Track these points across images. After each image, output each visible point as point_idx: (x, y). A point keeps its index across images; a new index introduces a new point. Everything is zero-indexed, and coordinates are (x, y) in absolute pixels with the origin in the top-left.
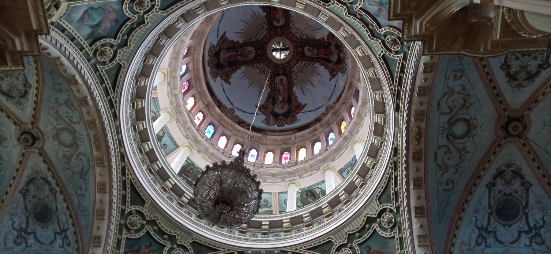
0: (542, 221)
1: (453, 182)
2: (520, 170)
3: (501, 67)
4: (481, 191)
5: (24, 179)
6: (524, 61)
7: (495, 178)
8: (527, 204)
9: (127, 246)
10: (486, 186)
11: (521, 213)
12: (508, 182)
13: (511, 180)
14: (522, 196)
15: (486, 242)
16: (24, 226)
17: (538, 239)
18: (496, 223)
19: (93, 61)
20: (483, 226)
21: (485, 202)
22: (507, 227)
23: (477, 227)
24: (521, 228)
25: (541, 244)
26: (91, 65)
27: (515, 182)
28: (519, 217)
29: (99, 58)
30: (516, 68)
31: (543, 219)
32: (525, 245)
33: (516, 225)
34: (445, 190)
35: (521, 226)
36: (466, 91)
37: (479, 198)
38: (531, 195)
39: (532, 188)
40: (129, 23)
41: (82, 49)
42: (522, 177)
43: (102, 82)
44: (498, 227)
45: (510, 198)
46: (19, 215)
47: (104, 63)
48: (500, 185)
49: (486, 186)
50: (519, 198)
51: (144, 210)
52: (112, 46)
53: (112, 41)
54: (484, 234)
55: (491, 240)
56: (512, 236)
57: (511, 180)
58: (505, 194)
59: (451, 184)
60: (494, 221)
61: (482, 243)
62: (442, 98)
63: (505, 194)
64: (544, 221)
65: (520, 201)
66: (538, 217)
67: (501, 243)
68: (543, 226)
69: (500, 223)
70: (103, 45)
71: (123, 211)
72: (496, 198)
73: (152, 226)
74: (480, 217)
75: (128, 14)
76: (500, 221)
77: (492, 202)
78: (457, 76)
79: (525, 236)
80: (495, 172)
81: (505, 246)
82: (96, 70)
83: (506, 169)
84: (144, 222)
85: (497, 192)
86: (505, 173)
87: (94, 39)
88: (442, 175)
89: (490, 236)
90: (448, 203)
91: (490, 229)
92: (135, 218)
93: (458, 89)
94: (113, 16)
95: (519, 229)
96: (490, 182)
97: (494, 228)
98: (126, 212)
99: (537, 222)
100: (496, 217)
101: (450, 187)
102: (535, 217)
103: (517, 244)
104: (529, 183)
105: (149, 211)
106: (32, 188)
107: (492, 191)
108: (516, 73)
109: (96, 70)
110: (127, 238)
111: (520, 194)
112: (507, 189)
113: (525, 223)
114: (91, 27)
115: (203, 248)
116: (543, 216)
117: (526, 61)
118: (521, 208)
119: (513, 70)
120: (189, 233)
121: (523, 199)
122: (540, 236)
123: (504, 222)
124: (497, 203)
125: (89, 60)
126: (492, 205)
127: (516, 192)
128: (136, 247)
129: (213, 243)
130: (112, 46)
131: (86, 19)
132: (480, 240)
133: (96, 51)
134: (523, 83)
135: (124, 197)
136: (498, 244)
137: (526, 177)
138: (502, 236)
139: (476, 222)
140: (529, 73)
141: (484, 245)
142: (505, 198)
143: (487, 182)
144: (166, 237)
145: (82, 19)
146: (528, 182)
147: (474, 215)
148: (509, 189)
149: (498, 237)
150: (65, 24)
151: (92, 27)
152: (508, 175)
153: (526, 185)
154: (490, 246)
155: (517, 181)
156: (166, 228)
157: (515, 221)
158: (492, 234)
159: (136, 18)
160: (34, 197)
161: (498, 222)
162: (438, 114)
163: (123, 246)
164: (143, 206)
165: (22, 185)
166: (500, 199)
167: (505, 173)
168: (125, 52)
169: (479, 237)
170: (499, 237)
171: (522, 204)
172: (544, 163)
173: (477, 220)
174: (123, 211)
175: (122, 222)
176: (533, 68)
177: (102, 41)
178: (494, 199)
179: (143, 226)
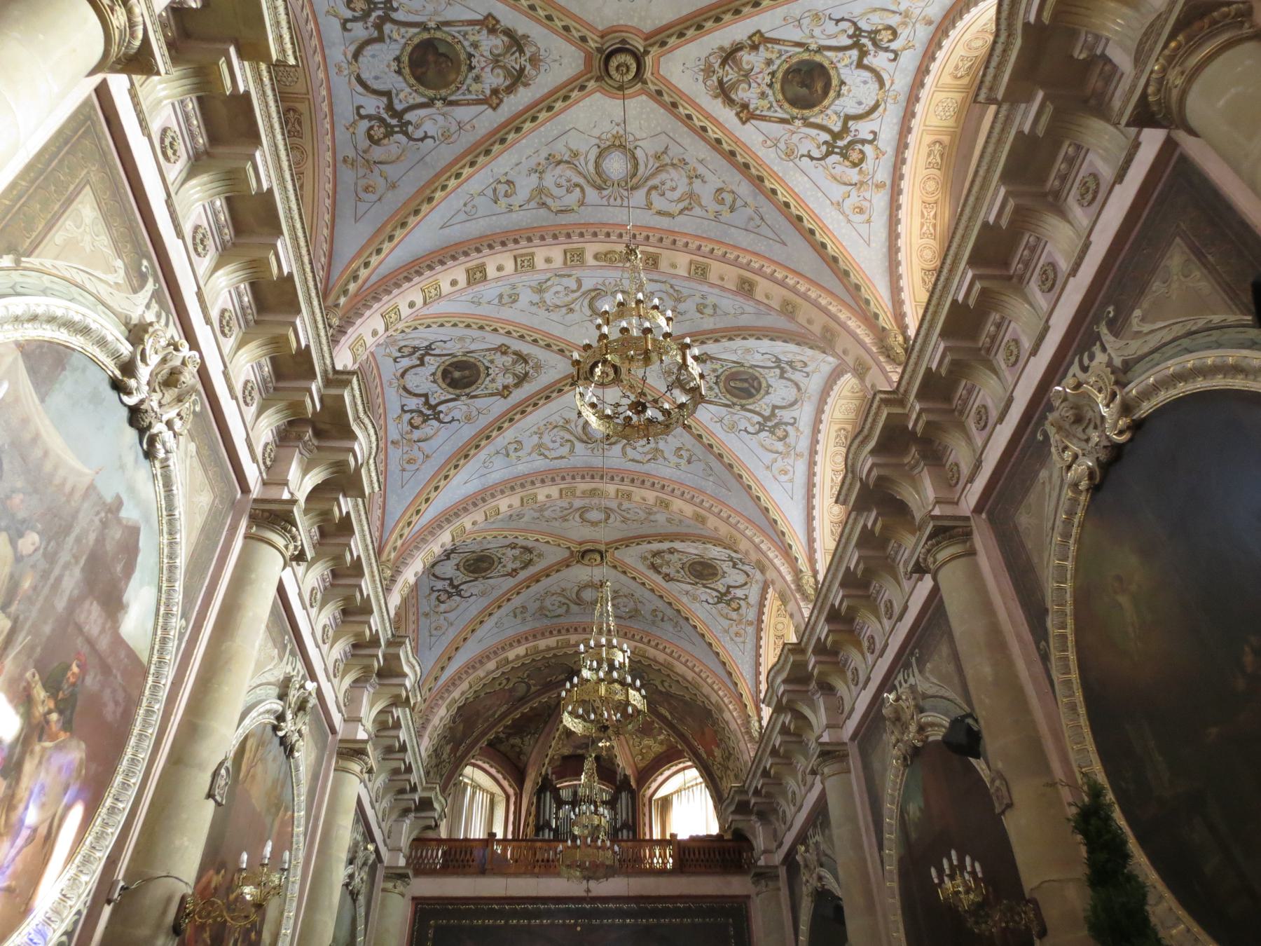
0: (422, 135)
2: (526, 85)
3: (759, 31)
6: (760, 76)
7: (508, 33)
8: (452, 103)
10: (490, 15)
11: (431, 93)
12: (497, 61)
13: (504, 67)
14: (470, 92)
15: (355, 19)
17: (379, 132)
18: (403, 41)
20: (396, 10)
22: (394, 66)
24: (397, 95)
25: (370, 137)
27: (498, 75)
28: (422, 89)
30: (748, 63)
31: (426, 137)
32: (359, 108)
33: (404, 85)
35: (402, 96)
39: (490, 110)
42: (510, 90)
45: (464, 68)
48: (490, 44)
49: (490, 15)
50: (465, 87)
54: (374, 15)
56: (376, 78)
57: (504, 67)
58: (470, 56)
60: (409, 35)
61: (354, 10)
63: (470, 56)
64: (422, 140)
65: (458, 88)
66: (429, 127)
67: (356, 56)
68: (410, 138)
72: (461, 38)
76: (409, 49)
79: (382, 106)
80: (520, 32)
83: (528, 55)
85: (476, 38)
89: (372, 30)
91: (388, 27)
95: (394, 91)
97: (390, 38)
99: (417, 127)
100: (416, 41)
102: (428, 121)
103: (360, 89)
104: (498, 105)
107: (477, 28)
108: (738, 64)
111: (474, 87)
112: (482, 59)
113: (411, 102)
116: (433, 137)
117: (759, 81)
118: (443, 92)
119: (746, 57)
121: (464, 94)
122: (387, 135)
123: (405, 59)
124: (449, 39)
126: (445, 29)
127: (477, 79)
134: (715, 78)
136: (352, 48)
137: (512, 96)
138: (373, 56)
140: (734, 86)
142: (463, 56)
143: (499, 17)
146: (501, 101)
148: (483, 64)
149: (369, 48)
152: (512, 61)
153: (493, 99)
154: (345, 28)
155: (501, 80)
157: (412, 81)
158: (376, 34)
166: (458, 47)
170: (369, 50)
171: (453, 93)
172: (542, 129)
176: (744, 94)
178: (459, 32)
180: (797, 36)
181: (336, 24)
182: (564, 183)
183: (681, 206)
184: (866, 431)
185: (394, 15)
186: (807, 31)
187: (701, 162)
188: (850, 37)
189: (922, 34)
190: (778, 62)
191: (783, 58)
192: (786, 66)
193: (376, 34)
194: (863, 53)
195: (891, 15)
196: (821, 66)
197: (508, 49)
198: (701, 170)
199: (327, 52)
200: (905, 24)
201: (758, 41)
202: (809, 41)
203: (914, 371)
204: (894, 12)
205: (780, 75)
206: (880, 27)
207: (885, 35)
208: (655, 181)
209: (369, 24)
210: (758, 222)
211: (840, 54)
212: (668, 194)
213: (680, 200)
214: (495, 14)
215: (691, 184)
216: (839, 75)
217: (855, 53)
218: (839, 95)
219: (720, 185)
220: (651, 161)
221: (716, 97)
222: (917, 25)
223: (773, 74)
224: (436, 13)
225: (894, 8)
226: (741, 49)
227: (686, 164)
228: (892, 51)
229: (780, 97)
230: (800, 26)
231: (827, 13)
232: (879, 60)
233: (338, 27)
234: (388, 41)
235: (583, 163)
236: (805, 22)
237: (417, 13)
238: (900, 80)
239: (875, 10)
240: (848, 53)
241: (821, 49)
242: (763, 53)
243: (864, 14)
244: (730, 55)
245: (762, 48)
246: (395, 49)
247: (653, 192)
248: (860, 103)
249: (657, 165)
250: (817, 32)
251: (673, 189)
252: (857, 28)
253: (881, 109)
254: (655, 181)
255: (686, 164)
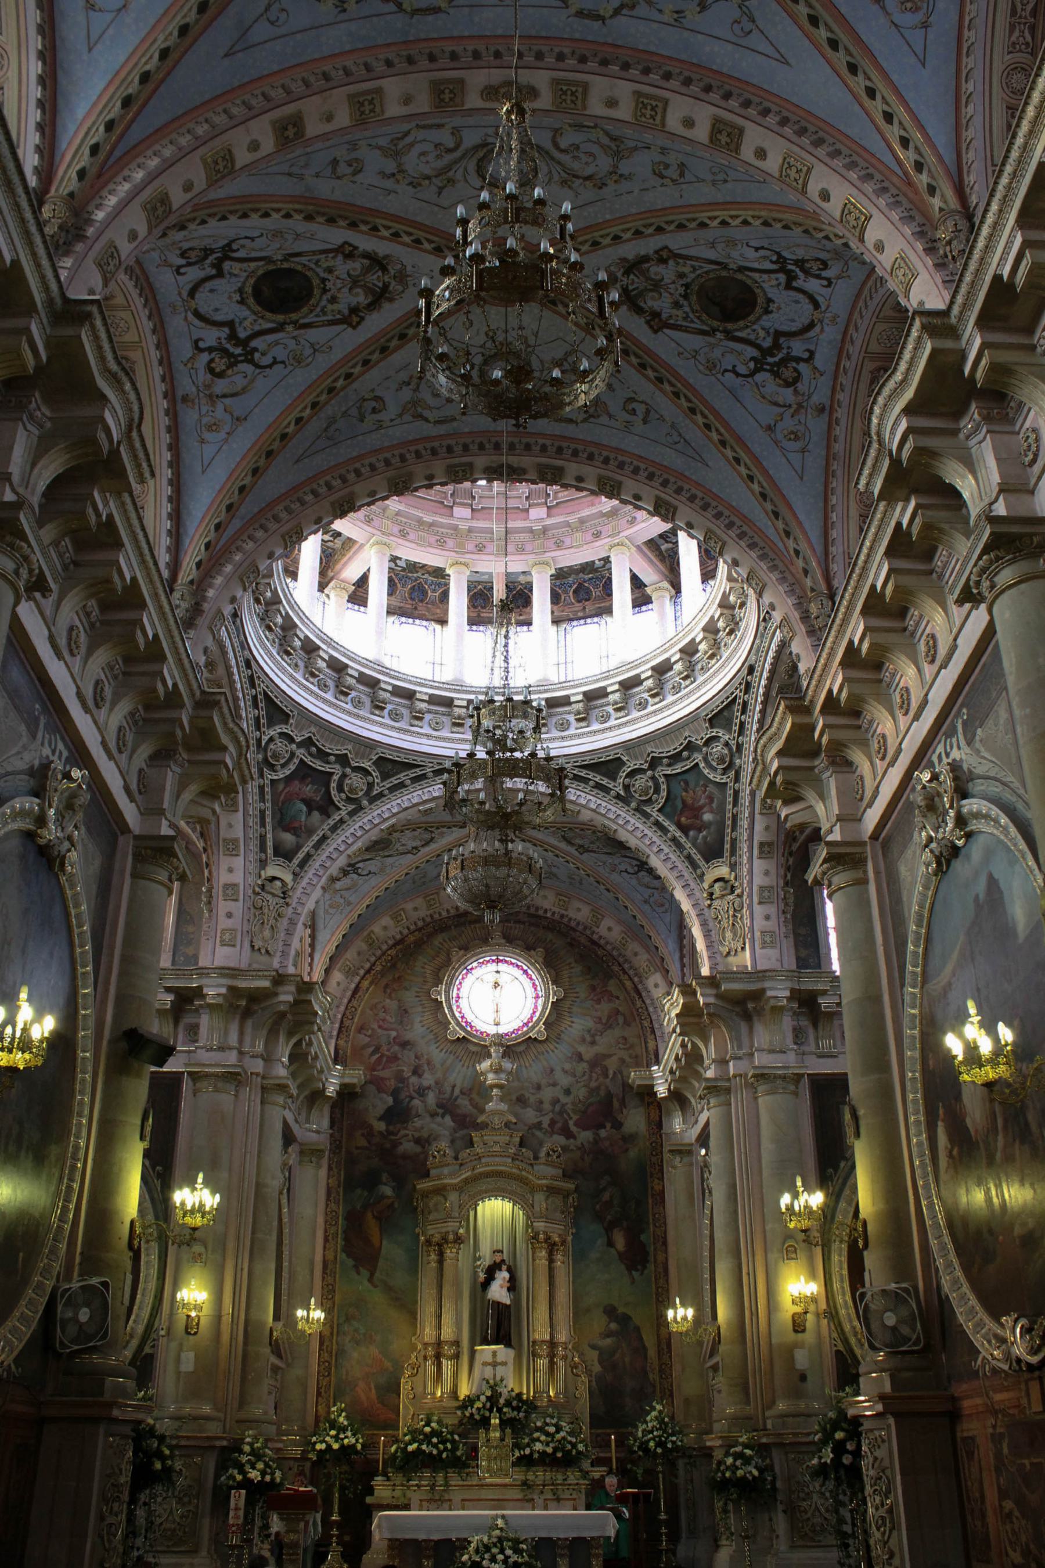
1: (631, 400)
3: (354, 328)
4: (664, 345)
5: (563, 845)
9: (668, 816)
10: (656, 332)
11: (739, 276)
12: (655, 285)
15: (798, 360)
16: (635, 863)
19: (365, 803)
20: (752, 359)
21: (696, 342)
22: (772, 307)
23: (752, 374)
26: (371, 803)
28: (749, 282)
29: (361, 794)
34: (645, 421)
35: (774, 283)
36: (411, 377)
37: (679, 354)
38: (692, 252)
40: (308, 760)
41: (342, 821)
43: (402, 785)
44: (767, 325)
46: (616, 862)
47: (370, 786)
48: (662, 303)
49: (656, 332)
51: (631, 765)
52: (344, 776)
53: (336, 777)
54: (776, 359)
55: (798, 348)
56: (797, 302)
57: (648, 279)
58: (685, 296)
59: (634, 405)
60: (749, 330)
61: (796, 370)
62: (427, 420)
63: (685, 296)
67: (811, 325)
69: (759, 319)
70: (340, 789)
71: (618, 797)
72: (691, 315)
73: (661, 764)
74: (728, 362)
75: (292, 767)
76: (751, 318)
77: (698, 325)
78: (374, 409)
81: (821, 321)
82: (381, 795)
84: (649, 773)
85: (674, 312)
86: (631, 288)
87: (326, 807)
88: (610, 416)
90: (673, 426)
91: (767, 343)
92: (641, 782)
93: (406, 394)
94: (296, 785)
96: (648, 322)
97: (768, 333)
98: (622, 793)
100: (741, 323)
101: (641, 409)
105: (636, 759)
106: (578, 841)
108: (368, 290)
109: (381, 795)
110: (659, 810)
111: (686, 270)
114: (309, 813)
115: (725, 713)
118: (724, 273)
119: (361, 298)
120: (691, 719)
123: (758, 310)
124: (704, 317)
125: (361, 808)
128: (680, 805)
129: (723, 695)
130: (344, 776)
131: (296, 825)
132: (788, 374)
133: (349, 800)
134: (392, 272)
135: (598, 786)
136: (812, 334)
137: (642, 253)
139: (738, 375)
141: (802, 367)
142: (694, 298)
144: (685, 754)
145: (295, 831)
147: (719, 376)
150: (301, 855)
151: (310, 810)
154: (812, 353)
156: (674, 746)
158: (782, 340)
159: (301, 753)
160: (592, 843)
161: (754, 323)
162: (464, 418)
163: (666, 823)
164: (623, 764)
165: (572, 850)
166: (697, 307)
167: (631, 288)
168: (356, 754)
169: (776, 375)
170: (794, 327)
173: (734, 371)
174: (618, 797)
175: (633, 805)
177: (333, 792)
178: (692, 322)
179: (653, 778)
180: (312, 335)
181: (818, 361)
182: (582, 155)
183: (409, 139)
184: (134, 434)
185: (755, 353)
186: (303, 342)
187: (389, 192)
188: (256, 350)
189: (186, 386)
190: (324, 303)
191: (318, 309)
192: (313, 301)
193: (782, 340)
194: (233, 336)
195: (226, 391)
196: (272, 311)
197: (641, 294)
198: (389, 184)
199: (840, 337)
200: (208, 387)
201: (353, 317)
202: (296, 333)
203: (128, 519)
204: (225, 396)
205: (316, 292)
206: (230, 372)
207: (220, 365)
208: (448, 158)
209: (785, 351)
210: (295, 170)
211: (257, 328)
212: (429, 147)
213: (411, 145)
214: (649, 331)
215: (400, 165)
216: (249, 308)
217: (242, 334)
218: (240, 291)
219: (359, 178)
220: (459, 176)
221: (387, 257)
222: (194, 389)
223: (325, 291)
224: (712, 346)
225: (227, 401)
226: (369, 305)
227: (411, 183)
228: (202, 350)
229: (309, 274)
230: (312, 345)
231: (290, 368)
232: (212, 336)
233: (817, 356)
234: (772, 331)
235: (554, 171)
236: (308, 351)
237: (732, 351)
238: (177, 324)
239: (244, 390)
240: (249, 332)
241: (280, 328)
242: (342, 306)
243: (253, 381)
244: (380, 297)
245: (346, 312)
246: (766, 321)
247: (452, 145)
248: (212, 291)
249: (451, 174)
250: (291, 344)
251: (423, 154)
252: (251, 361)
253: (185, 294)
254: (448, 158)
255: (411, 183)
